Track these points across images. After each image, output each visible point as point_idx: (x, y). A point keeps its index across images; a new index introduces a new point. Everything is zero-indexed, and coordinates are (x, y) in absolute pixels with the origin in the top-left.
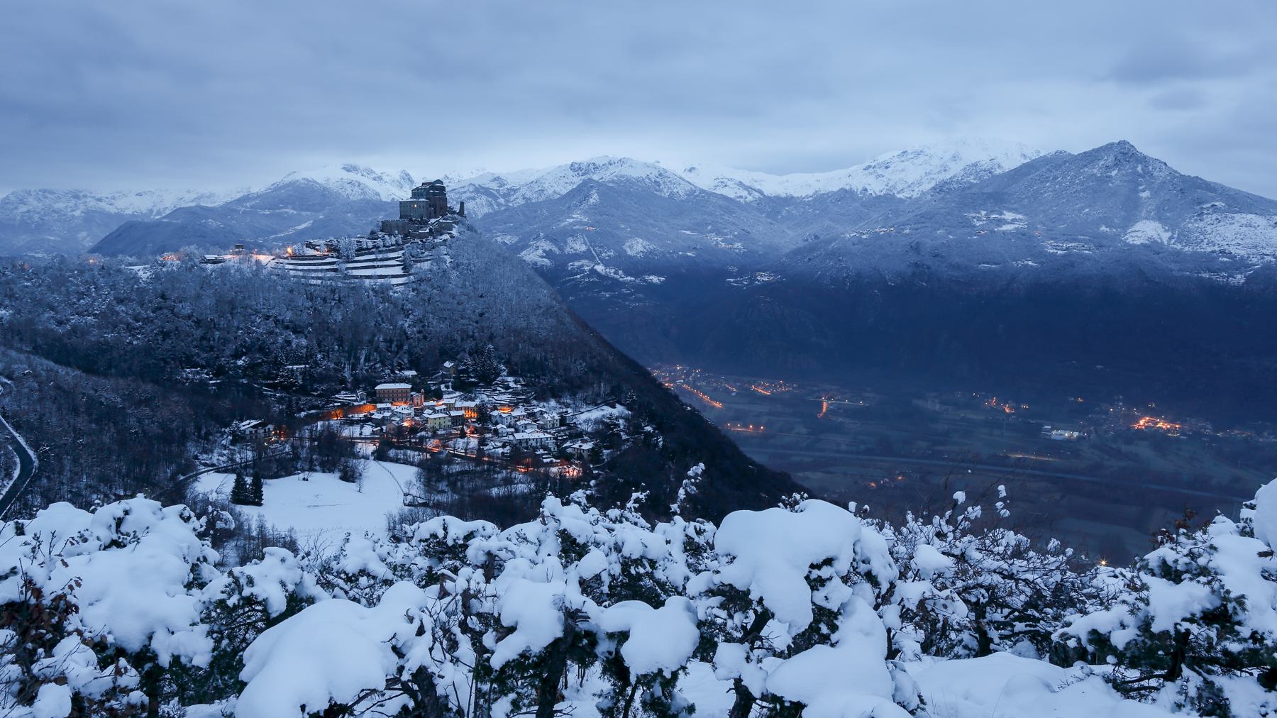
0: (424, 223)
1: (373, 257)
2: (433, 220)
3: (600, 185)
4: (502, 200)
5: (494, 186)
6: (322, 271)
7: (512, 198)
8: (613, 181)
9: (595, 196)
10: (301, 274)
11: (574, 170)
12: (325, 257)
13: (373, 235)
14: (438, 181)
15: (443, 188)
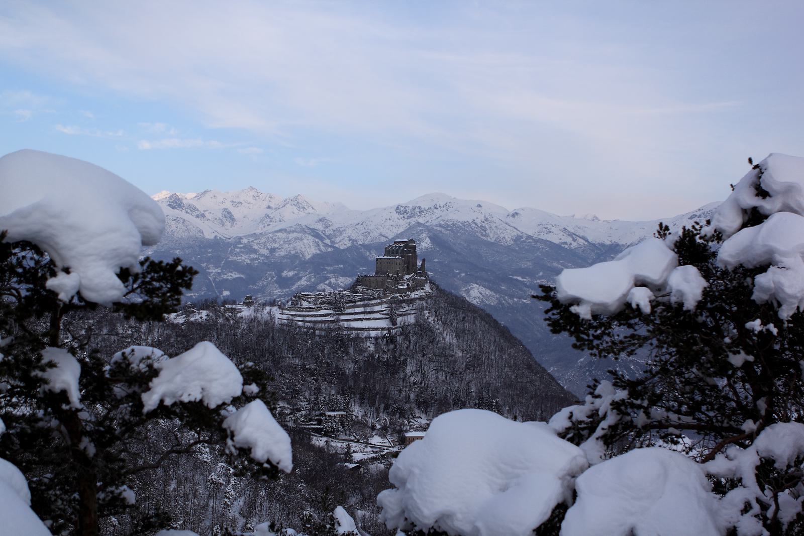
0: (400, 279)
1: (361, 309)
2: (407, 277)
3: (429, 229)
4: (328, 241)
5: (320, 227)
6: (325, 322)
7: (338, 240)
8: (440, 226)
9: (428, 240)
10: (309, 325)
11: (400, 213)
12: (320, 309)
13: (353, 288)
14: (412, 241)
15: (415, 247)
